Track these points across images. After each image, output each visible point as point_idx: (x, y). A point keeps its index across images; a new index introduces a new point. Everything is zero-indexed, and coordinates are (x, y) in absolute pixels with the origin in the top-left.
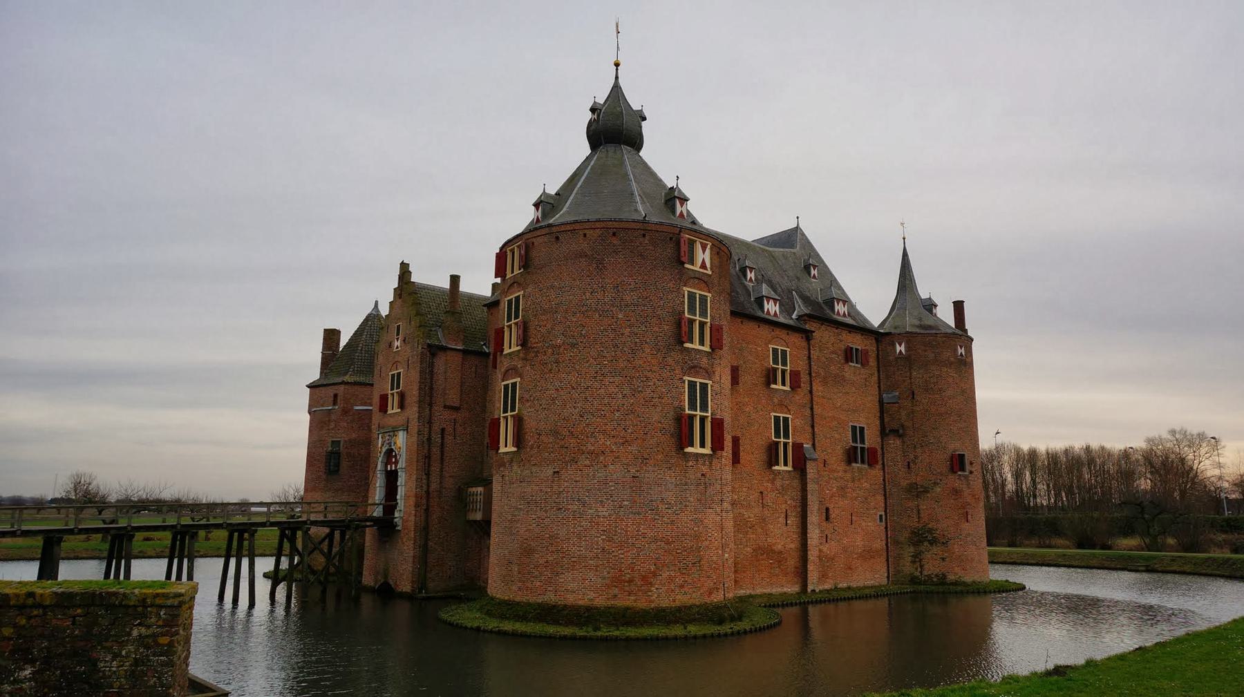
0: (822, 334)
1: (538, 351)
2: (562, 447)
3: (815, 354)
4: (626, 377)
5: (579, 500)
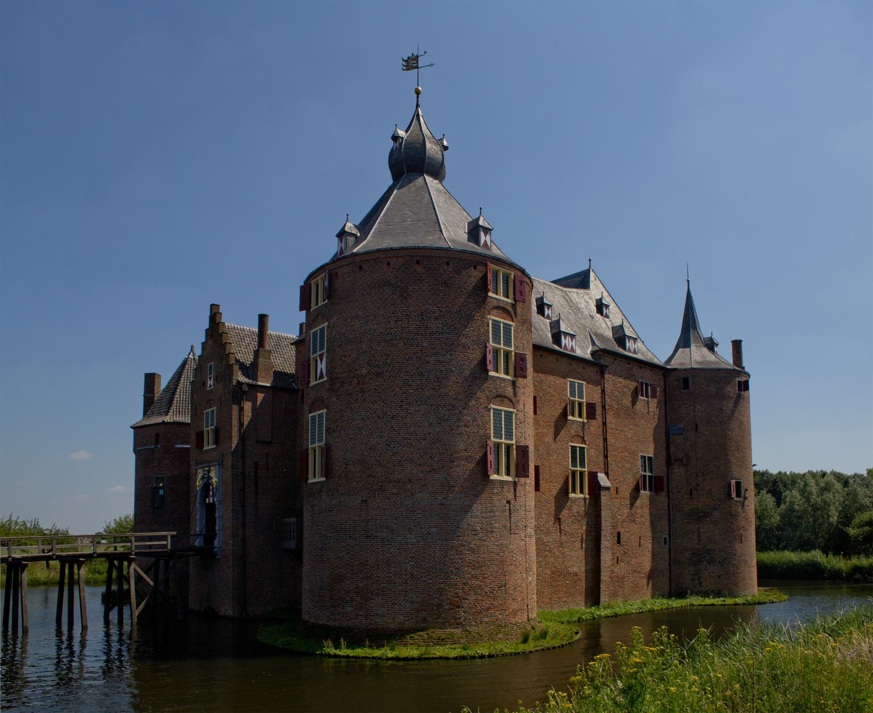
1: (343, 382)
3: (609, 387)
4: (432, 405)
5: (387, 527)
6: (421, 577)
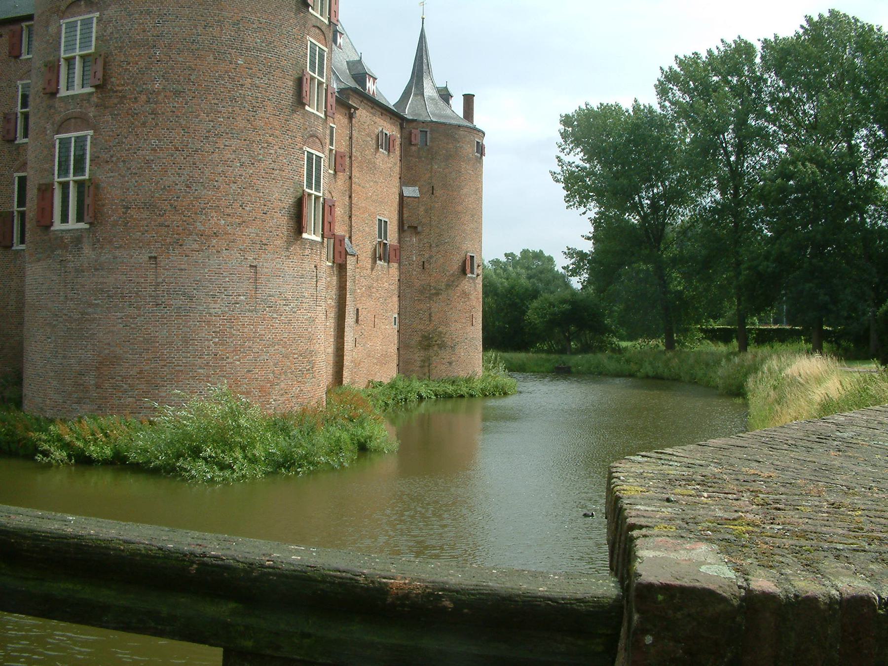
0: (363, 114)
2: (161, 225)
5: (184, 294)
6: (228, 358)
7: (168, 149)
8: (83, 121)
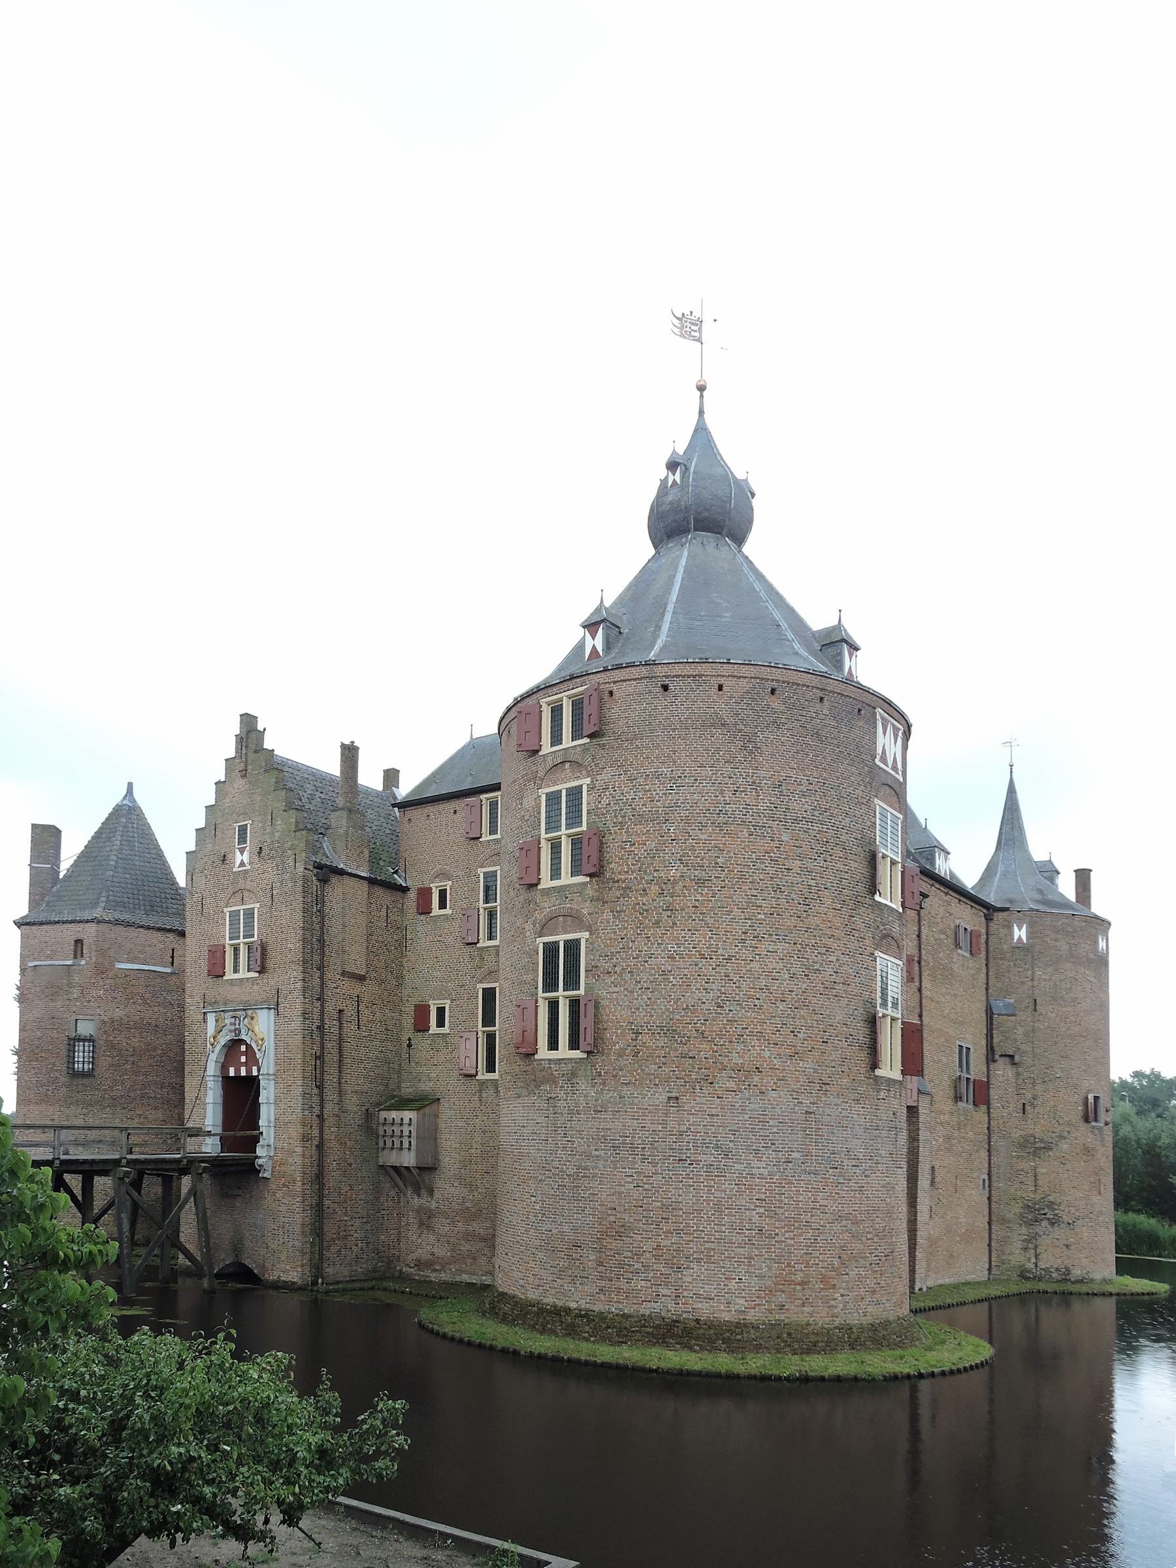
7: (690, 956)
8: (575, 920)
